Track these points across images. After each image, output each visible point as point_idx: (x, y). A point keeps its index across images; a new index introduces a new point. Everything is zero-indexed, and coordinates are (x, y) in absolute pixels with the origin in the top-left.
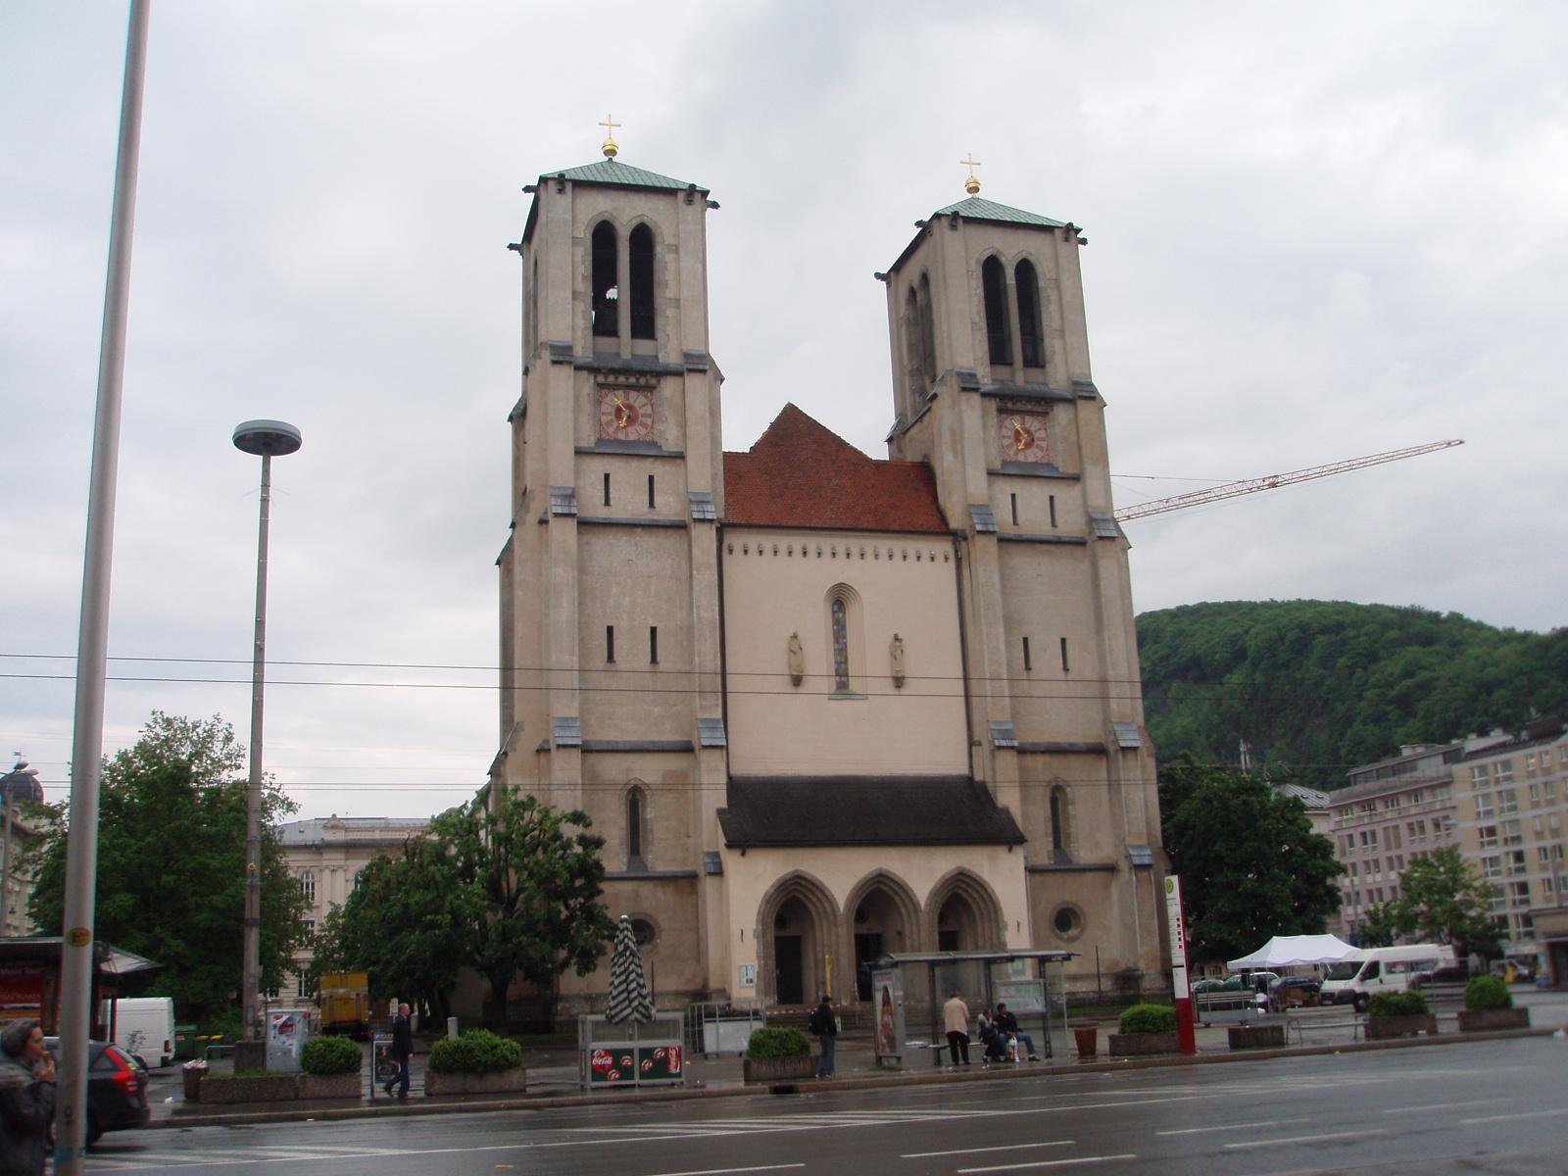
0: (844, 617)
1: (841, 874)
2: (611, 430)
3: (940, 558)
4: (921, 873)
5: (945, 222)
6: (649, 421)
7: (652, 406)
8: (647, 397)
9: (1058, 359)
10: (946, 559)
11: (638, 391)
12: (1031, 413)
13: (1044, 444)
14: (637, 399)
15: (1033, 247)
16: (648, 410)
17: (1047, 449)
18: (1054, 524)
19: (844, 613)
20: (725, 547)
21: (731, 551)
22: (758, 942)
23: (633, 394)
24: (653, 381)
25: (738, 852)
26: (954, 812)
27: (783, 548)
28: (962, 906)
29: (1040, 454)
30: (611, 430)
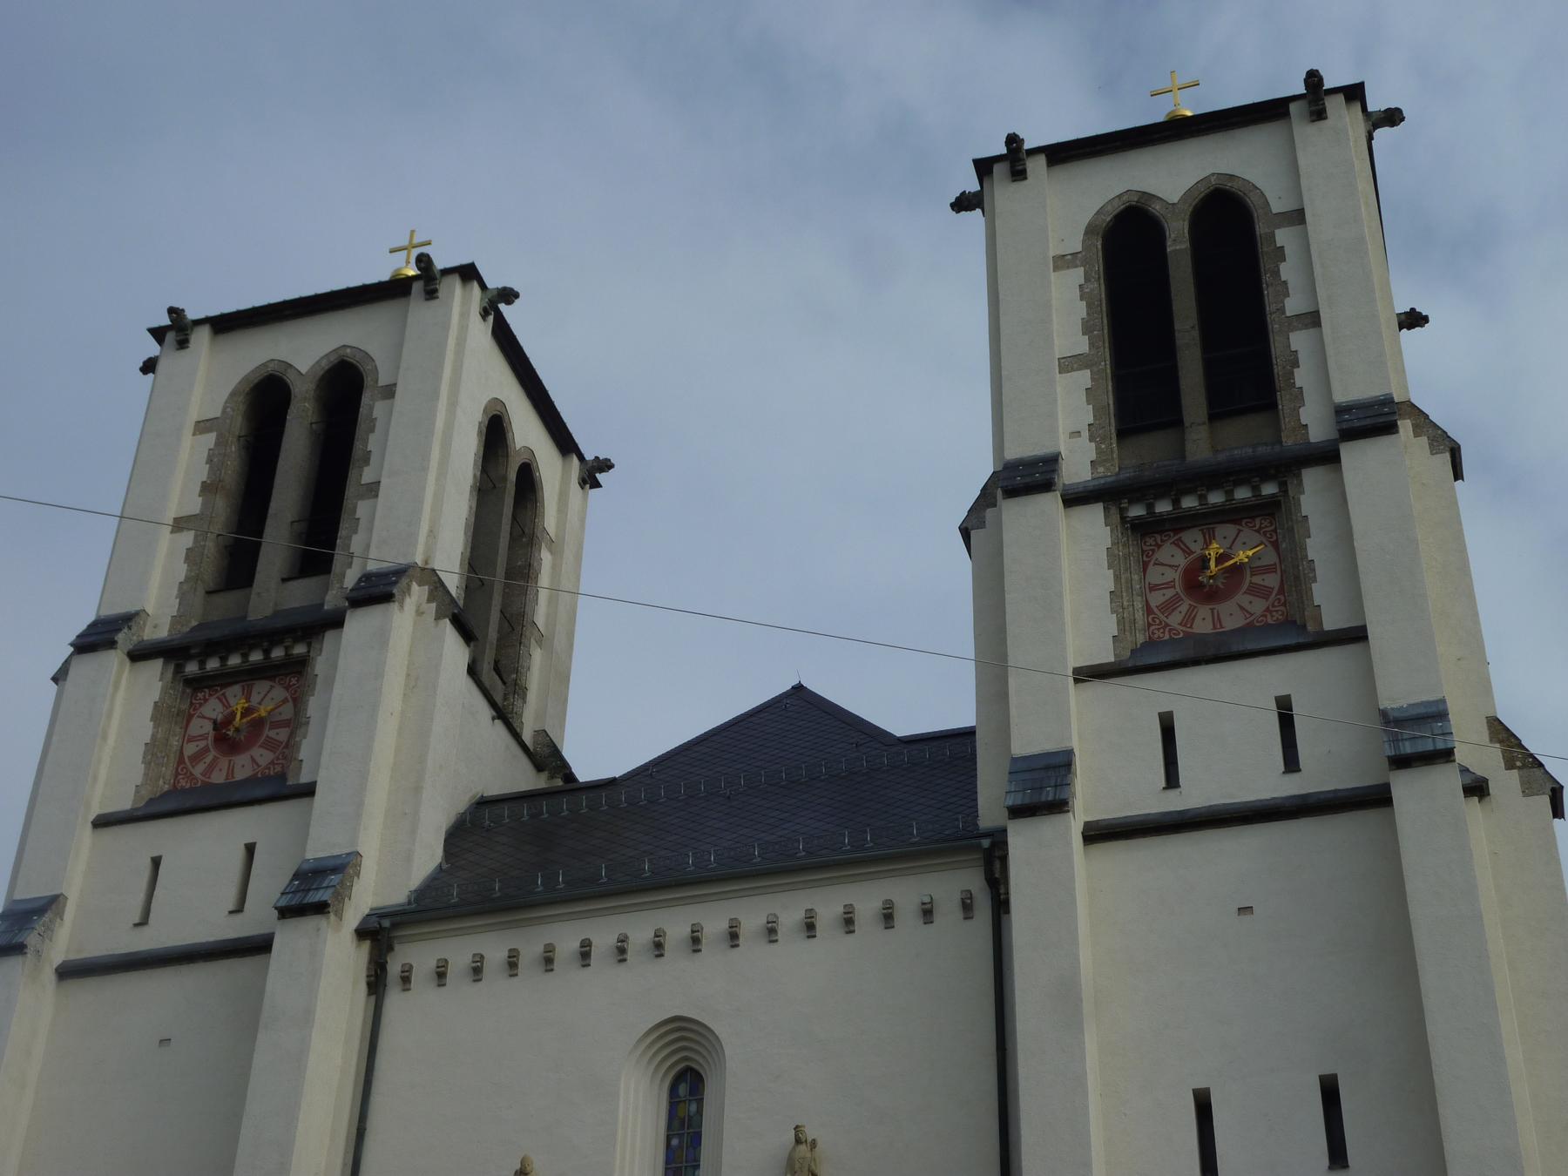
0: (700, 1112)
2: (198, 770)
3: (948, 910)
5: (999, 170)
6: (282, 735)
7: (295, 700)
8: (287, 688)
9: (1303, 377)
10: (967, 907)
11: (271, 678)
12: (1233, 514)
13: (1272, 581)
14: (267, 698)
15: (1243, 160)
16: (287, 711)
17: (1281, 591)
18: (1291, 762)
19: (700, 1101)
20: (394, 968)
21: (406, 980)
23: (260, 687)
24: (299, 649)
27: (531, 950)
29: (1258, 606)
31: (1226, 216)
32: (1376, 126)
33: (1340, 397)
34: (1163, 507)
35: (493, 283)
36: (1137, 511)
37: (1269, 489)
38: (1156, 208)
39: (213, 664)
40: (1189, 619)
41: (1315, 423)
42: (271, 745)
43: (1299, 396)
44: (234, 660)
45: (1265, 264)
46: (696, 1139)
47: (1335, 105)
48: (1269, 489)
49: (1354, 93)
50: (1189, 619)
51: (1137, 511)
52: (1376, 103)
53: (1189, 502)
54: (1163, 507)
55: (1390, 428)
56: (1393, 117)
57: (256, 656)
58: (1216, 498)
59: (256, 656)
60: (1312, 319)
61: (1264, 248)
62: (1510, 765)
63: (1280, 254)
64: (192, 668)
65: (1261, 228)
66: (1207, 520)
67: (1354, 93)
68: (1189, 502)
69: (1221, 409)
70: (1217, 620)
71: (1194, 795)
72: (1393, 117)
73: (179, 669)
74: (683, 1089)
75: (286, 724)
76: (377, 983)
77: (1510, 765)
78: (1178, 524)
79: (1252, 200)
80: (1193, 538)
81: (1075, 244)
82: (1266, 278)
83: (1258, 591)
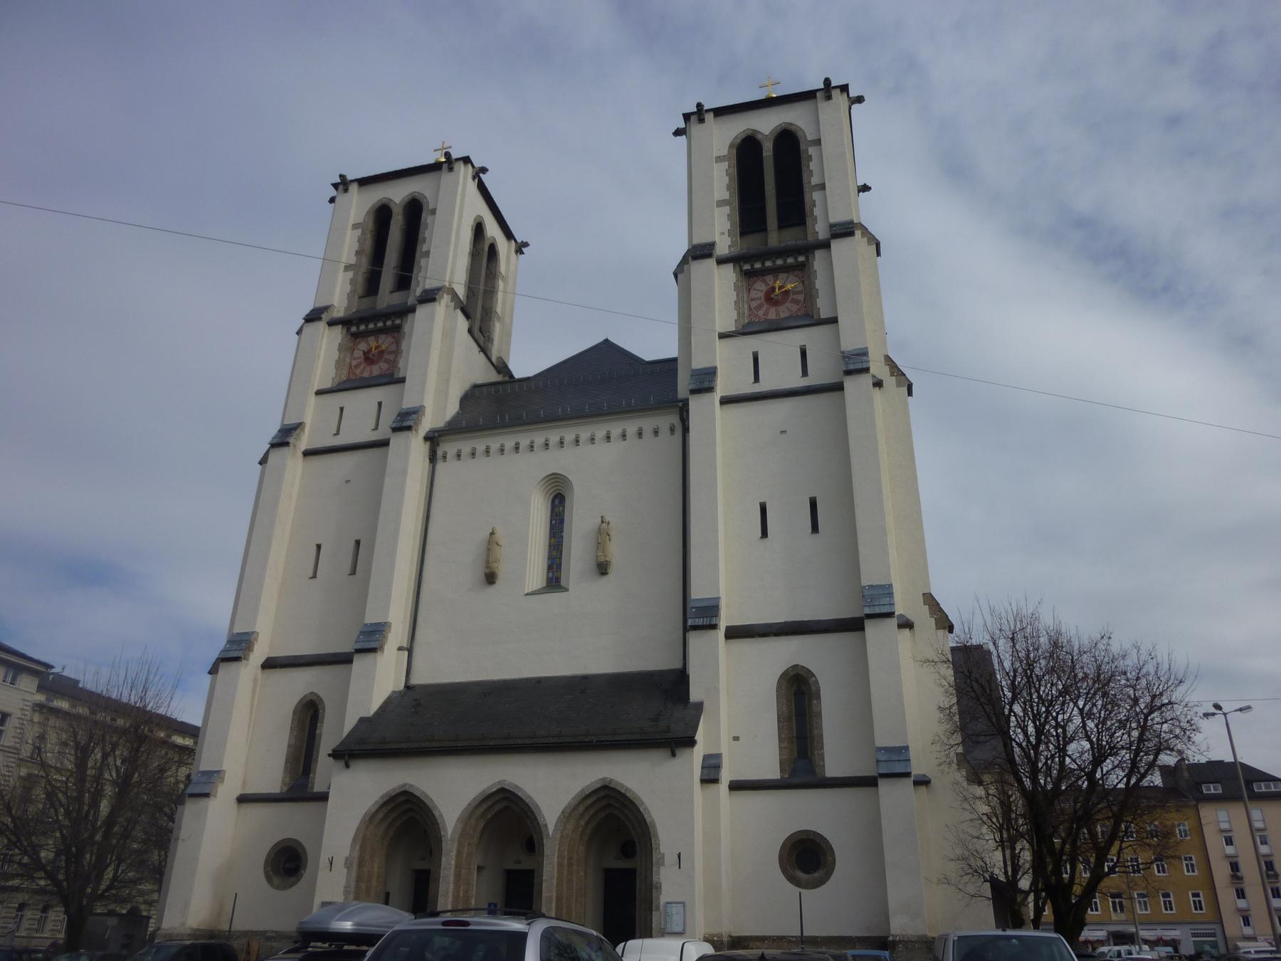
1: (452, 789)
4: (553, 787)
5: (693, 118)
6: (391, 357)
9: (817, 211)
10: (672, 430)
12: (786, 269)
13: (801, 297)
14: (385, 342)
16: (393, 347)
20: (440, 453)
21: (445, 457)
22: (349, 873)
23: (382, 337)
24: (398, 322)
25: (341, 764)
26: (655, 709)
28: (618, 832)
29: (795, 308)
30: (358, 372)
31: (788, 140)
32: (853, 103)
33: (832, 220)
34: (758, 265)
35: (477, 165)
36: (747, 267)
37: (801, 259)
38: (759, 137)
39: (362, 327)
40: (766, 313)
41: (821, 230)
42: (387, 361)
43: (815, 219)
44: (371, 326)
45: (804, 163)
46: (562, 521)
47: (836, 93)
48: (801, 259)
49: (844, 88)
50: (766, 313)
51: (747, 267)
52: (853, 93)
53: (768, 264)
54: (758, 265)
55: (851, 234)
56: (860, 100)
57: (380, 324)
58: (779, 262)
59: (380, 324)
60: (822, 187)
61: (803, 156)
62: (892, 375)
63: (810, 158)
64: (354, 329)
65: (803, 147)
66: (775, 271)
67: (844, 88)
68: (768, 264)
69: (783, 224)
70: (778, 314)
71: (765, 385)
72: (860, 100)
73: (348, 329)
74: (557, 502)
75: (393, 352)
76: (433, 458)
77: (892, 375)
78: (763, 273)
79: (800, 134)
80: (769, 279)
81: (725, 152)
82: (804, 168)
83: (795, 302)
